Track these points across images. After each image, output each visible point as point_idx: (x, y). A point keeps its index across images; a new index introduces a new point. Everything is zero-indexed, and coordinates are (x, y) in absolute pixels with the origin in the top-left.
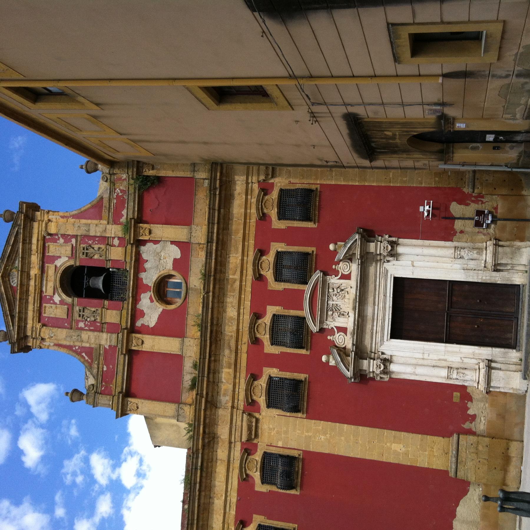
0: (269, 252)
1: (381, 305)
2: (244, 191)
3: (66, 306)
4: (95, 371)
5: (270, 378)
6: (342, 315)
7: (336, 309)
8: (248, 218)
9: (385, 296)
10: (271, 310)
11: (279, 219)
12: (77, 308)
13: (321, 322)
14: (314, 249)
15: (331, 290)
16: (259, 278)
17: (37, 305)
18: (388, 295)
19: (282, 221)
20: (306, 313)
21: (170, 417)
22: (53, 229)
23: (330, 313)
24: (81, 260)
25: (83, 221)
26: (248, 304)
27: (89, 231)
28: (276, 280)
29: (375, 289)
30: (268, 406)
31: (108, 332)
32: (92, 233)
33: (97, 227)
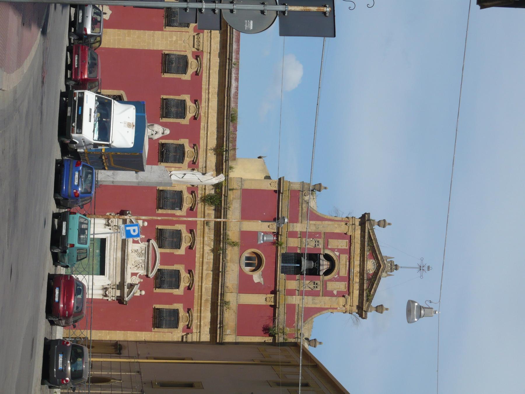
0: (185, 288)
1: (112, 258)
2: (202, 328)
3: (329, 247)
4: (304, 205)
5: (181, 209)
6: (136, 251)
7: (140, 255)
8: (199, 310)
9: (110, 264)
10: (182, 251)
11: (178, 310)
12: (321, 246)
13: (148, 246)
14: (155, 291)
15: (143, 266)
16: (190, 272)
17: (352, 248)
18: (108, 265)
19: (176, 308)
20: (158, 251)
21: (247, 180)
22: (342, 300)
23: (143, 252)
24: (319, 280)
25: (318, 306)
26: (197, 255)
27: (313, 300)
28: (179, 271)
29: (116, 267)
30: (181, 192)
31: (297, 232)
32: (310, 298)
33: (309, 302)
